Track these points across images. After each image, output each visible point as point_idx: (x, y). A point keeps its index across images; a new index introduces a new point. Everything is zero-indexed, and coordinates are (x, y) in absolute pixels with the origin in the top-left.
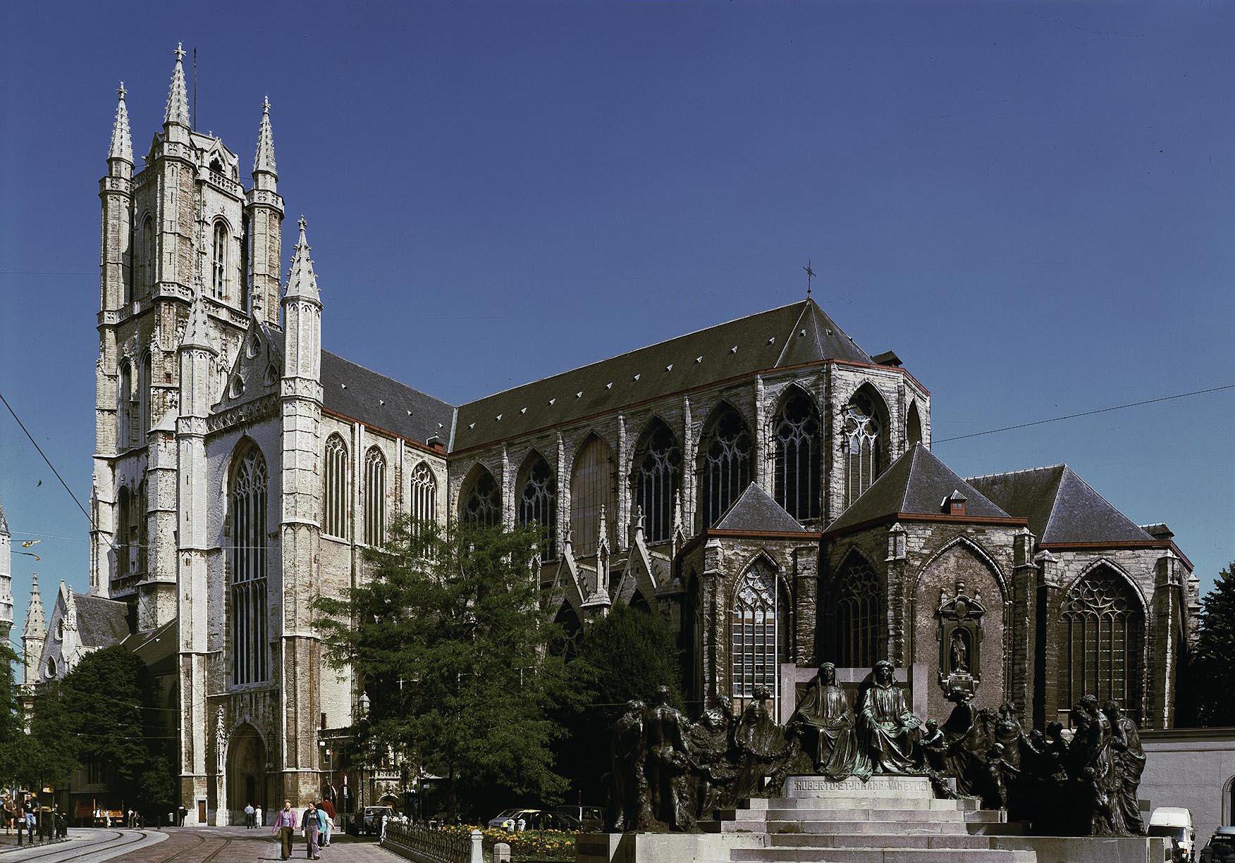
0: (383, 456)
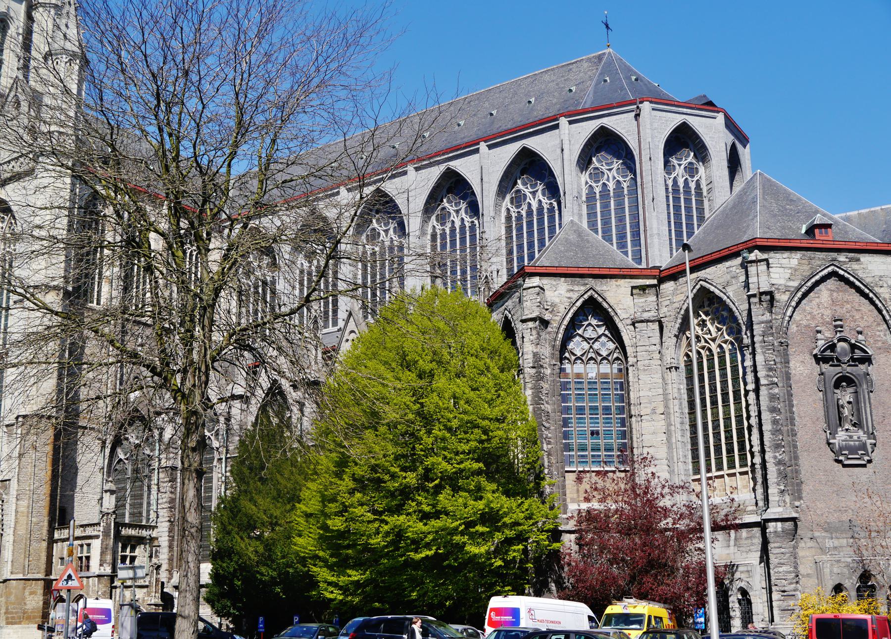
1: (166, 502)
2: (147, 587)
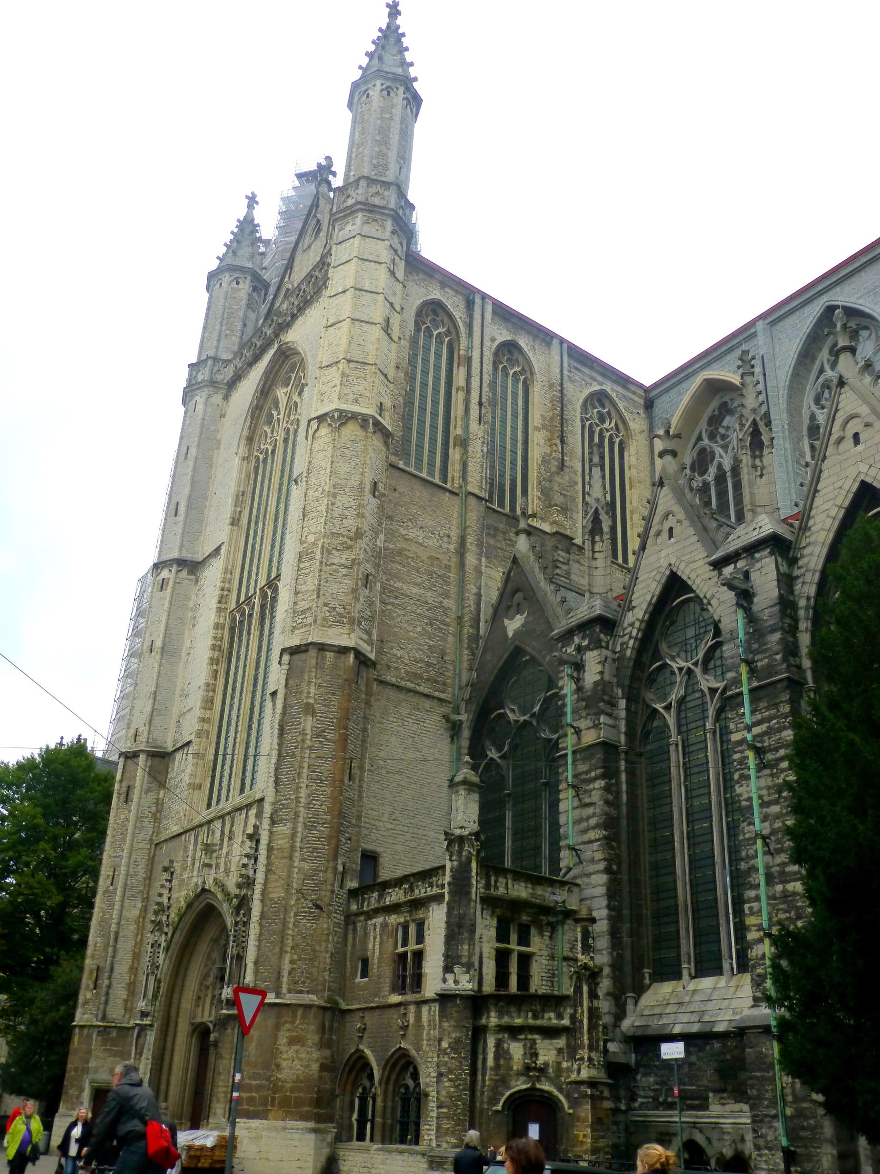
0: (528, 362)
1: (597, 826)
2: (565, 1030)
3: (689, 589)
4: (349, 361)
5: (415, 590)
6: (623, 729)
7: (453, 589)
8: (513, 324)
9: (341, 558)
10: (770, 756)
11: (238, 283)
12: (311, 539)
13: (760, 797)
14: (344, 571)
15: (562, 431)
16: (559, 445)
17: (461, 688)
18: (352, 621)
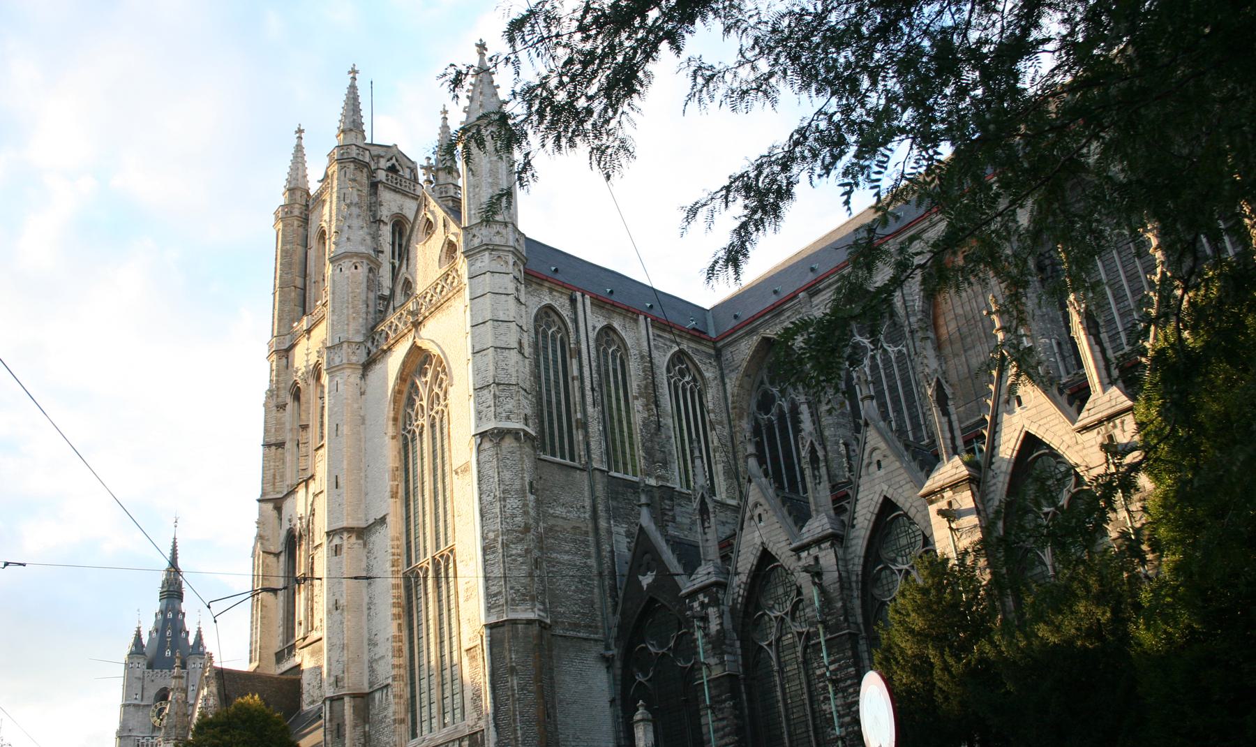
0: (622, 340)
3: (777, 561)
4: (498, 384)
5: (566, 557)
6: (740, 662)
7: (592, 550)
8: (608, 309)
9: (517, 549)
10: (842, 685)
11: (356, 268)
12: (491, 535)
13: (838, 711)
14: (520, 560)
15: (656, 396)
16: (655, 410)
17: (610, 629)
18: (533, 599)
